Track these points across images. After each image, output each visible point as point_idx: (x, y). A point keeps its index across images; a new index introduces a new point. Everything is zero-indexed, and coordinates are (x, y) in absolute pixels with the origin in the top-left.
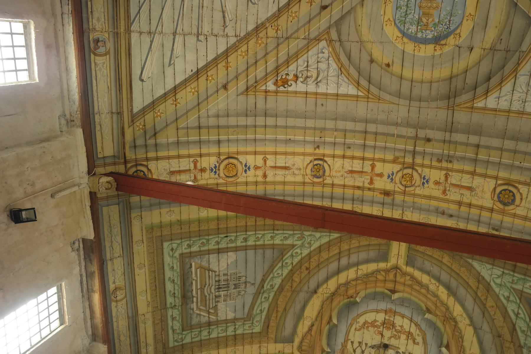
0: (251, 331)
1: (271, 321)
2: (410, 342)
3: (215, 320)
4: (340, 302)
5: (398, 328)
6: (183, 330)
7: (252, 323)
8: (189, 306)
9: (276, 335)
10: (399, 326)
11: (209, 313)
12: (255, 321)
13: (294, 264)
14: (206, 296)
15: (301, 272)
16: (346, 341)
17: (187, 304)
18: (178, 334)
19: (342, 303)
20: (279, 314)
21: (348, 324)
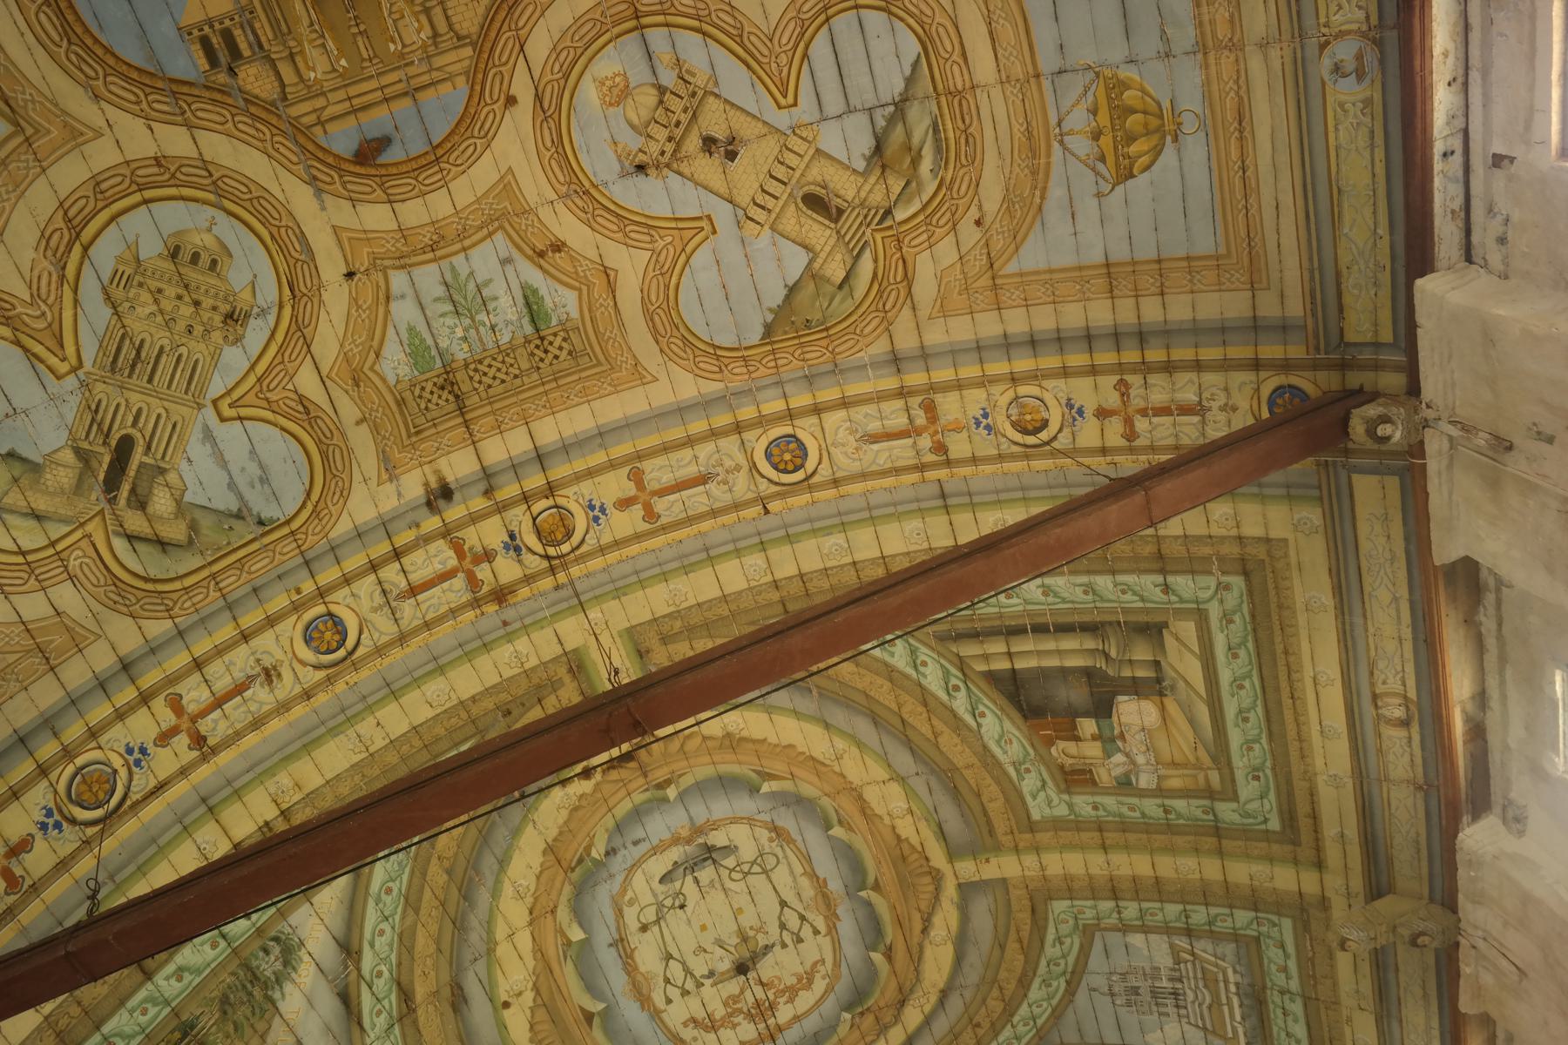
0: (1076, 903)
1: (1029, 921)
2: (700, 1014)
3: (1174, 937)
4: (882, 993)
5: (740, 1019)
6: (1257, 940)
7: (1076, 918)
8: (1246, 981)
9: (1008, 894)
10: (739, 1024)
11: (1193, 954)
12: (1071, 922)
13: (1009, 1026)
14: (1206, 986)
15: (988, 1016)
16: (832, 930)
17: (1251, 985)
18: (1269, 937)
19: (877, 994)
20: (1013, 935)
21: (844, 964)
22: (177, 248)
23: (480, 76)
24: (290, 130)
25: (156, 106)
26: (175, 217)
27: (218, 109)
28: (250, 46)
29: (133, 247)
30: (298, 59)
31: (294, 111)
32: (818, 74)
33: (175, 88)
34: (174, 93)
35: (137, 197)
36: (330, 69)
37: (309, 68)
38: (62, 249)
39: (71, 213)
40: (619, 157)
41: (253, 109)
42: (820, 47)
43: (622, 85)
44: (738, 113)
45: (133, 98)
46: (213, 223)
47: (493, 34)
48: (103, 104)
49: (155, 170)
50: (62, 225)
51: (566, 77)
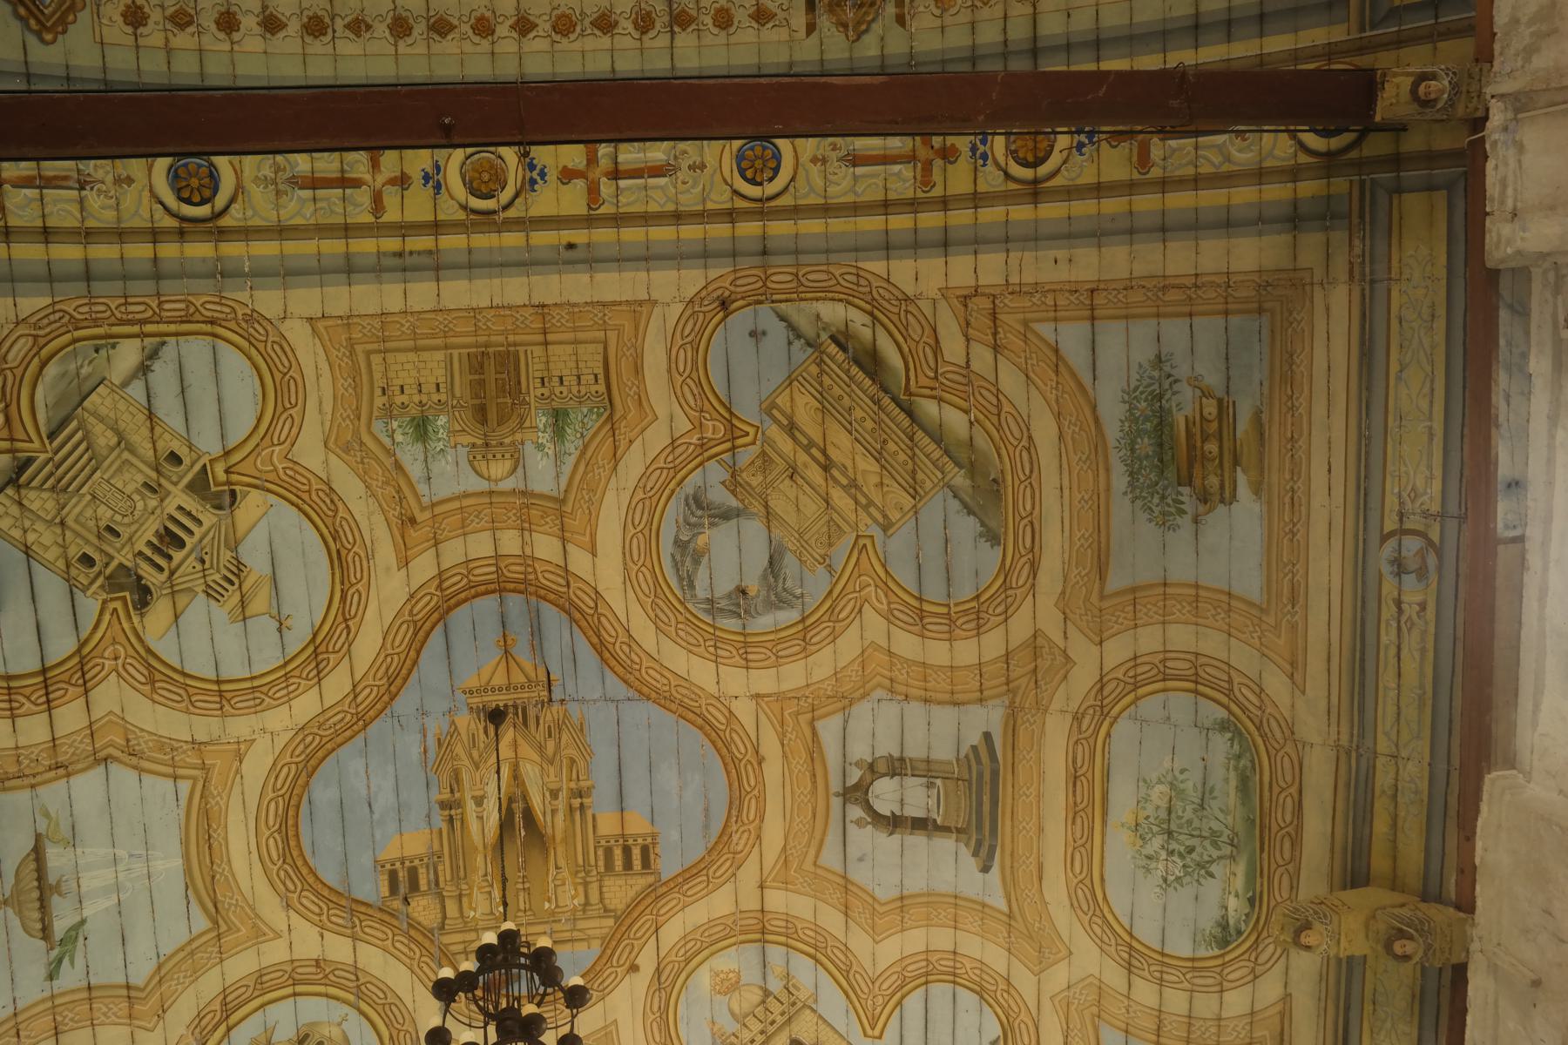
22: (307, 1036)
23: (614, 943)
24: (437, 953)
25: (333, 919)
26: (315, 1010)
27: (384, 929)
28: (429, 882)
29: (269, 1032)
30: (465, 900)
31: (446, 939)
32: (907, 1021)
33: (354, 906)
34: (352, 910)
35: (289, 990)
36: (488, 911)
37: (471, 908)
38: (210, 1027)
39: (228, 999)
40: (713, 1035)
41: (412, 933)
42: (914, 1003)
43: (733, 981)
44: (828, 1029)
45: (317, 910)
46: (345, 1019)
47: (635, 914)
48: (291, 911)
49: (313, 970)
50: (218, 1007)
51: (688, 961)
